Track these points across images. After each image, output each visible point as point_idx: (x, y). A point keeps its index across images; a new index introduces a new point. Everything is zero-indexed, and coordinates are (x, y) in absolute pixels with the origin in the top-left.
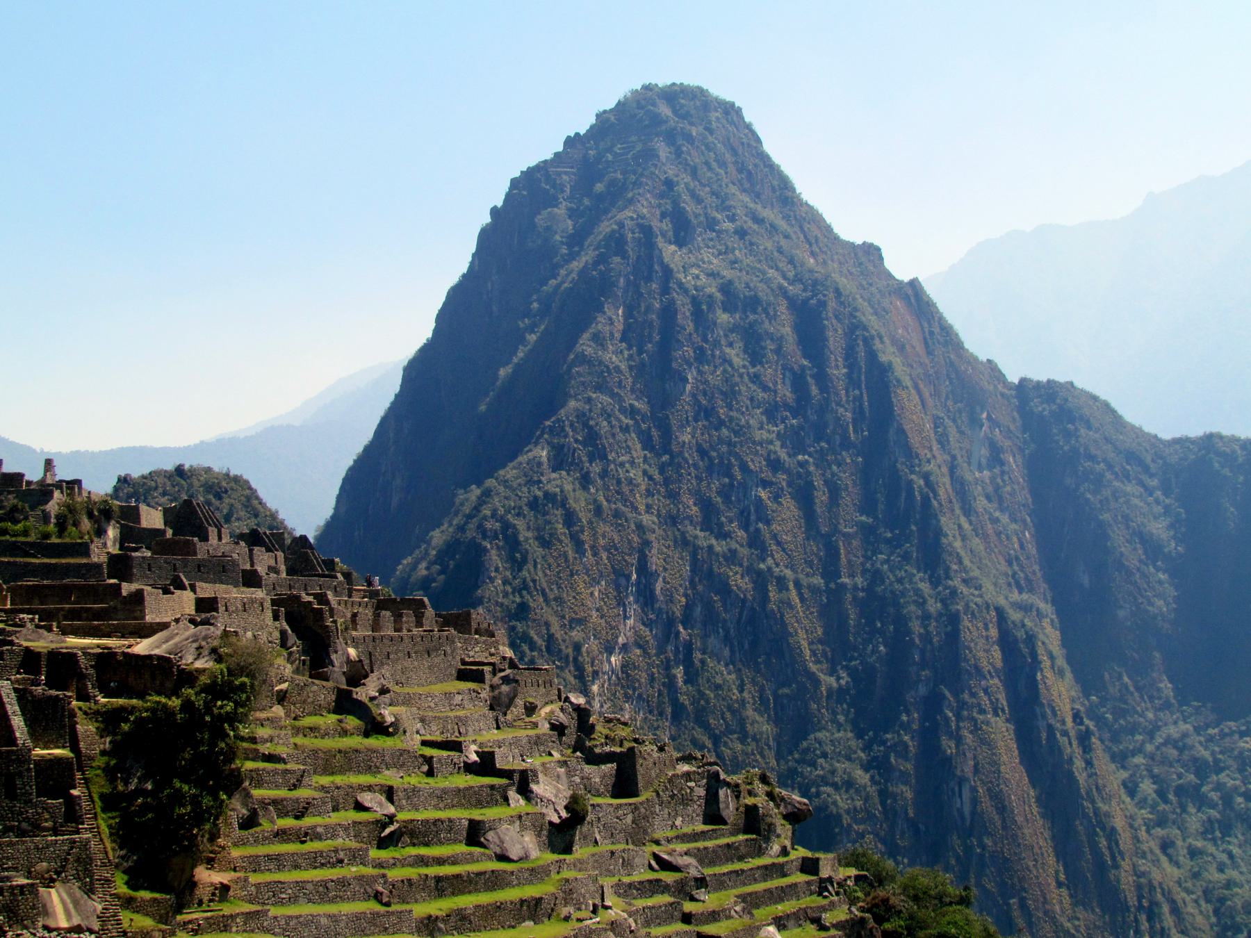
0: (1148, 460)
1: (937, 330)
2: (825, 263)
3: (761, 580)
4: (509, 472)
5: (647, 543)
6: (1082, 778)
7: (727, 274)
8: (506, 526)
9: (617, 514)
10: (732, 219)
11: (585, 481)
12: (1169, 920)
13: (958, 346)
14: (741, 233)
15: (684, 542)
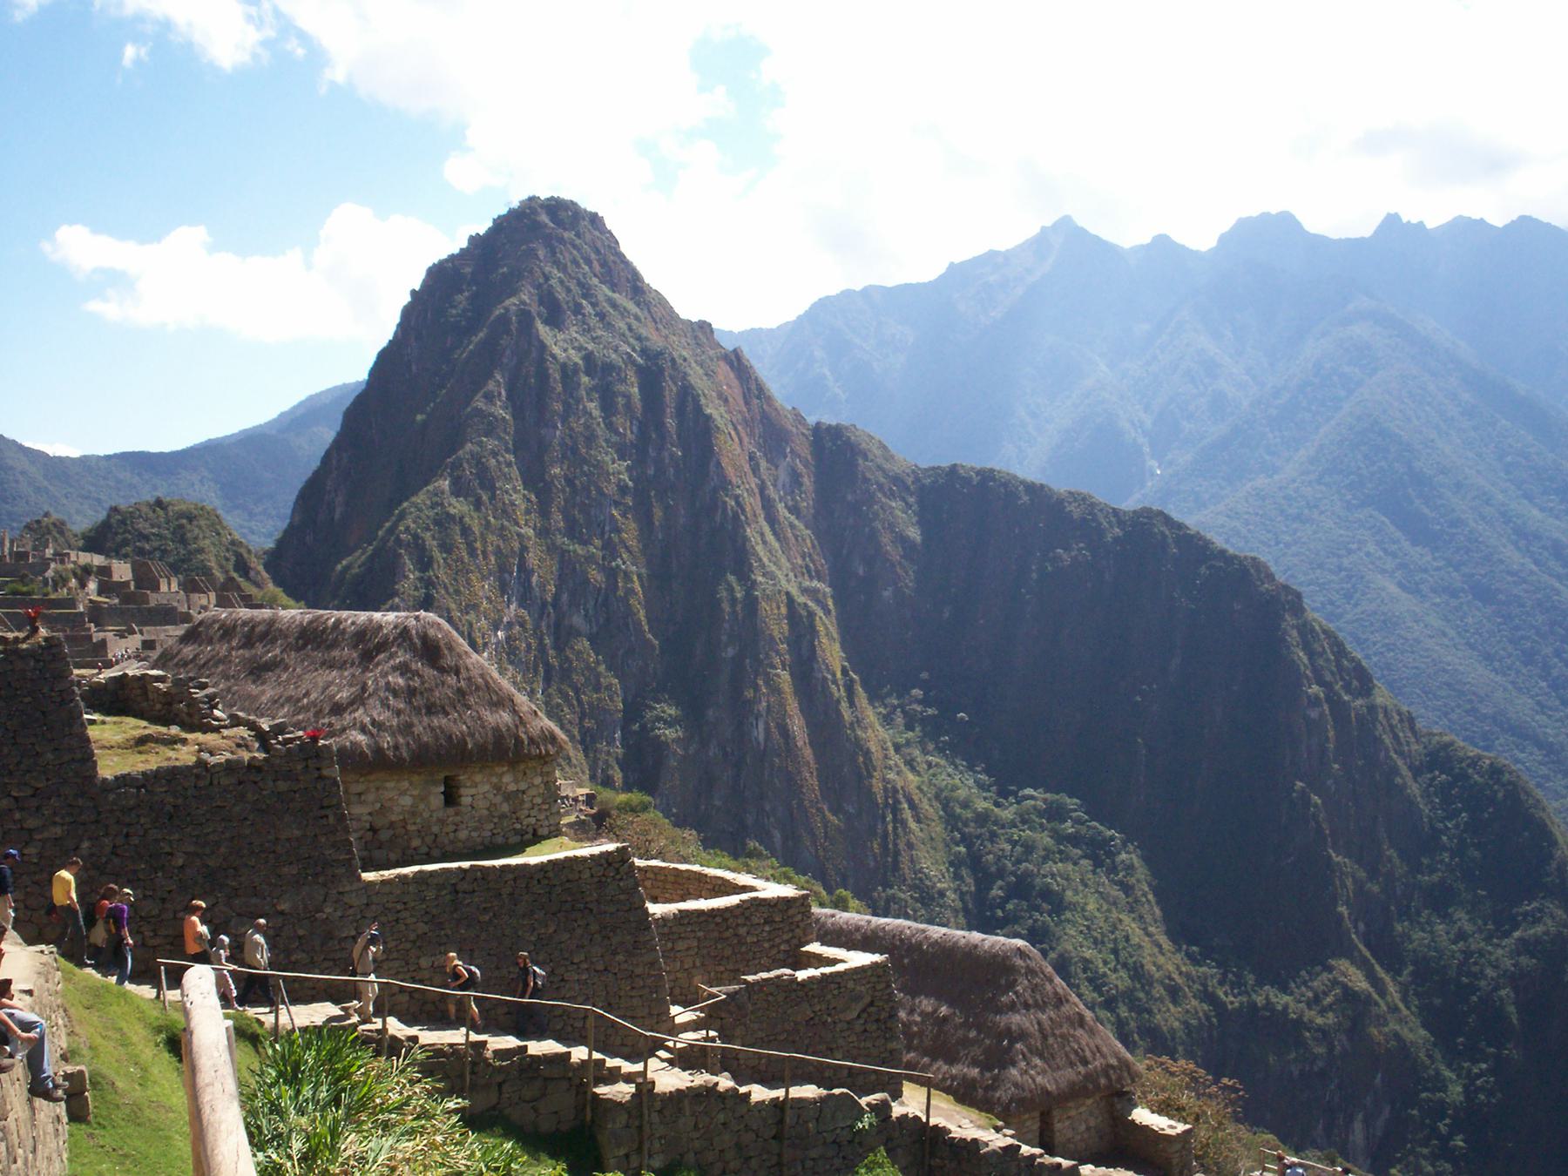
0: (909, 481)
1: (753, 387)
2: (666, 337)
3: (612, 574)
4: (420, 498)
5: (524, 549)
6: (847, 715)
7: (590, 346)
8: (416, 537)
9: (503, 528)
10: (594, 305)
11: (478, 505)
12: (908, 814)
13: (769, 399)
14: (602, 316)
15: (552, 549)
